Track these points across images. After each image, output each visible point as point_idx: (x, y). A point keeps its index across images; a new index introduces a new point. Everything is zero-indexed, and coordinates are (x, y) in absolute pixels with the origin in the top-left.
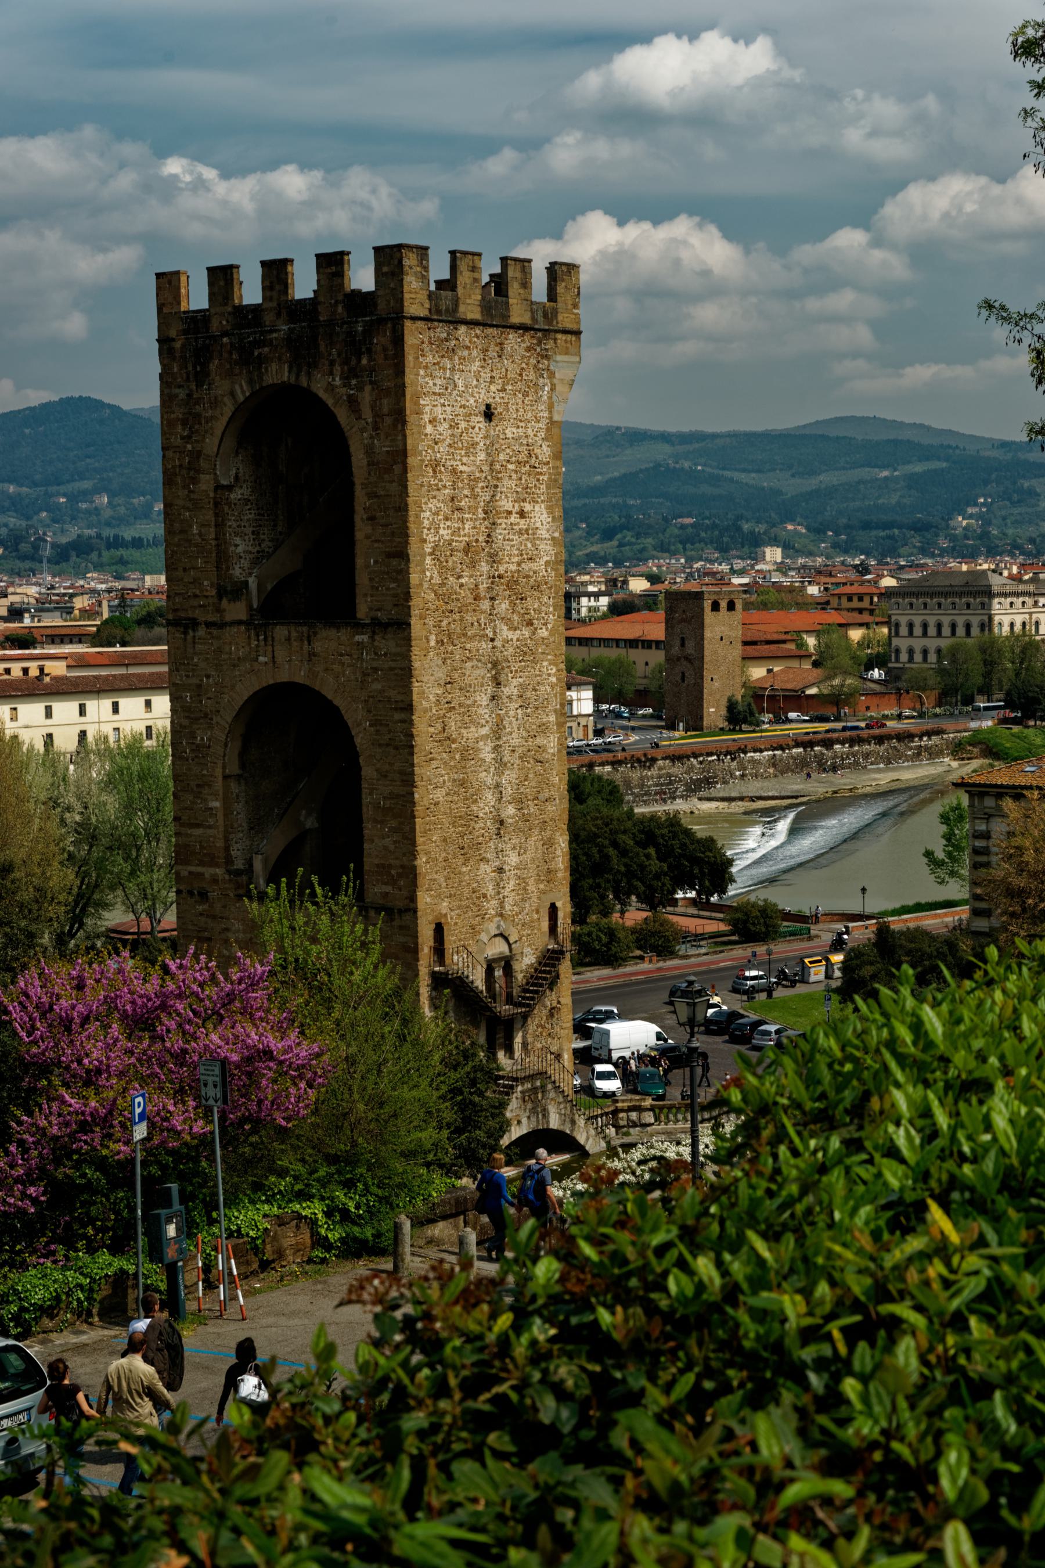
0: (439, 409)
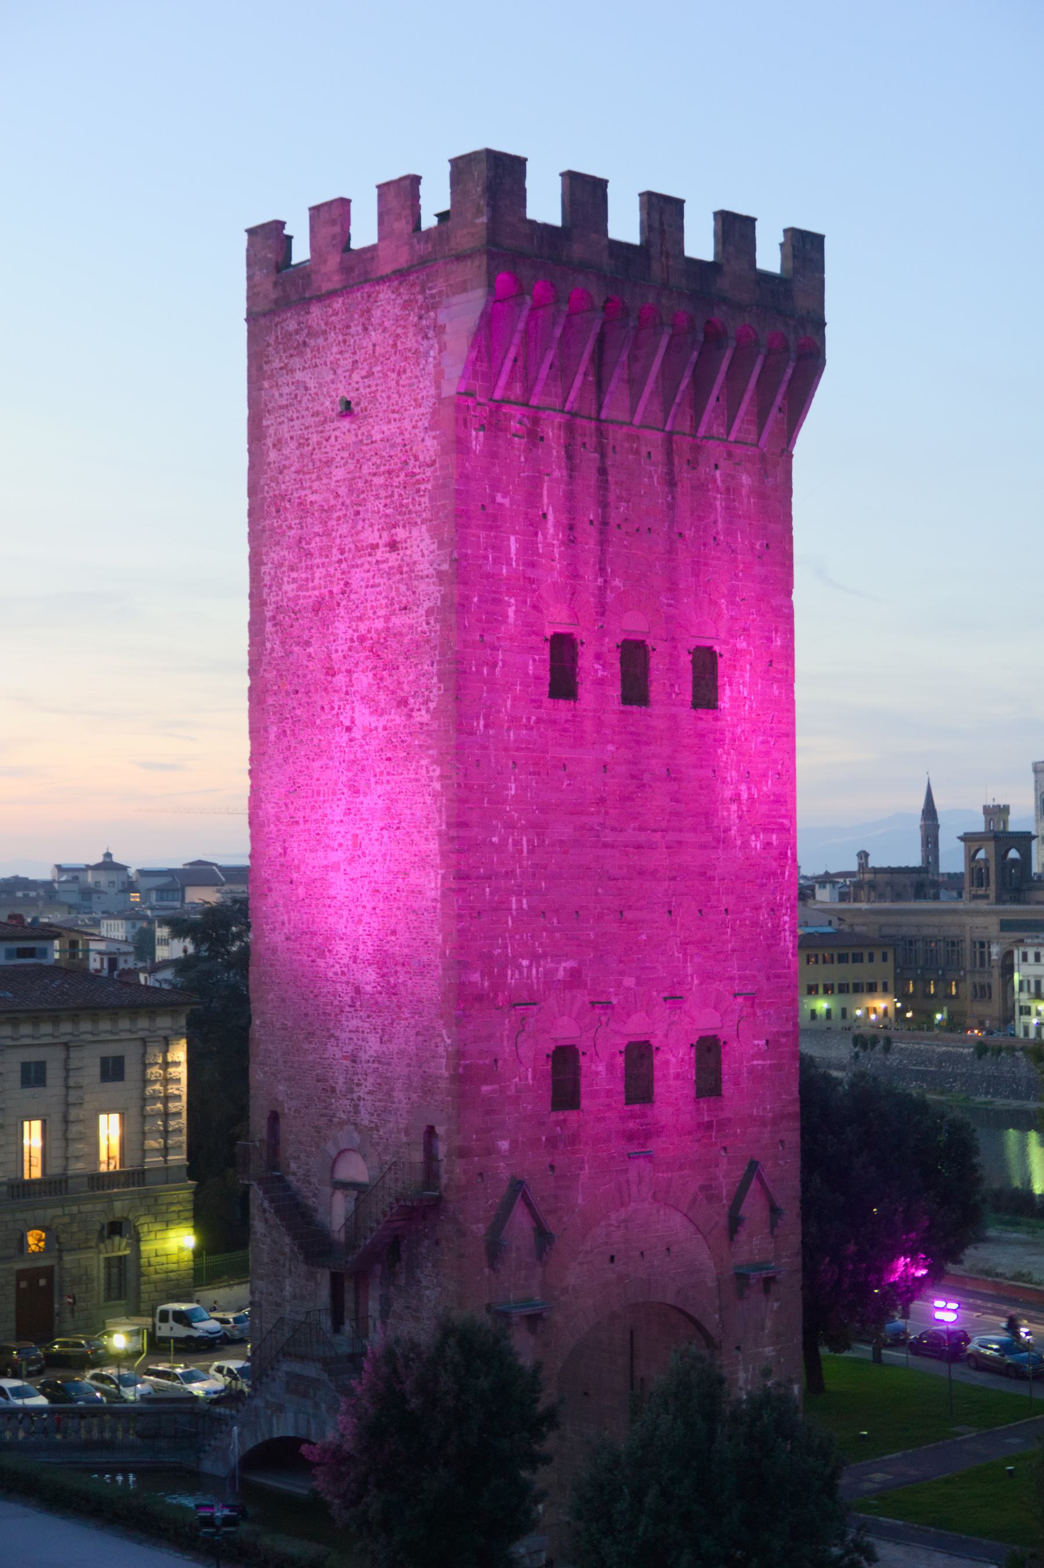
0: (285, 427)
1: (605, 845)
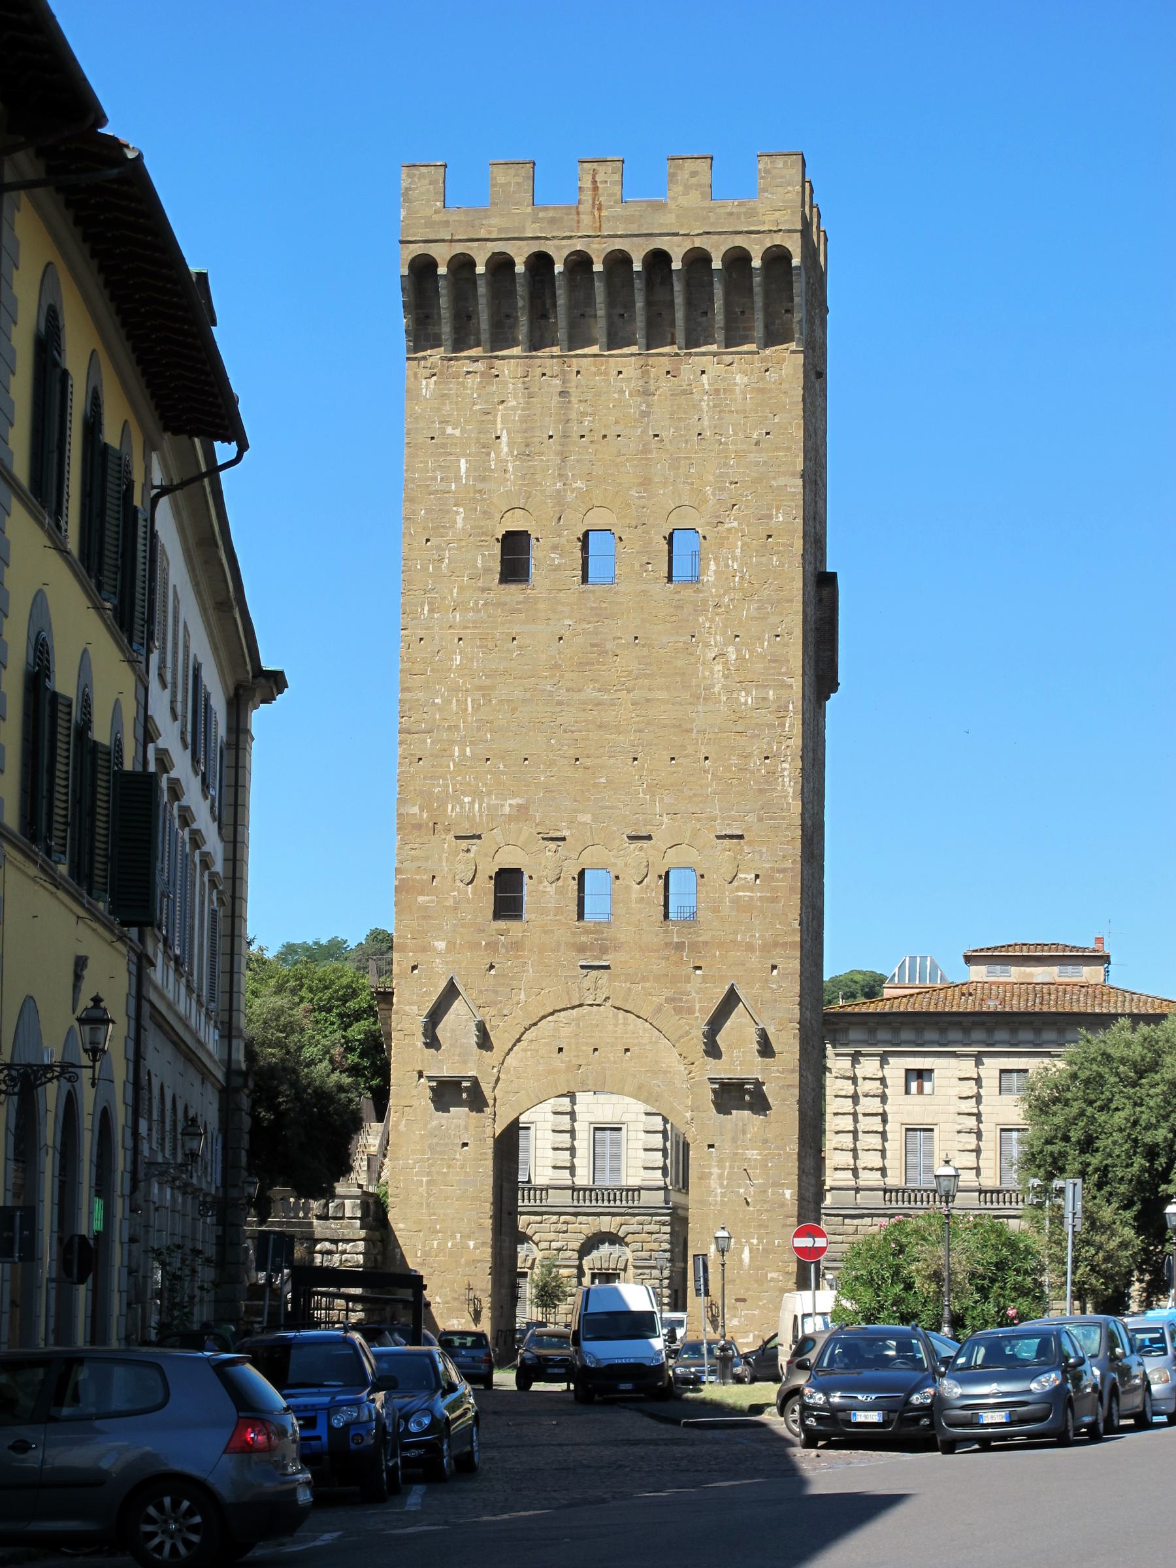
1: (560, 703)
